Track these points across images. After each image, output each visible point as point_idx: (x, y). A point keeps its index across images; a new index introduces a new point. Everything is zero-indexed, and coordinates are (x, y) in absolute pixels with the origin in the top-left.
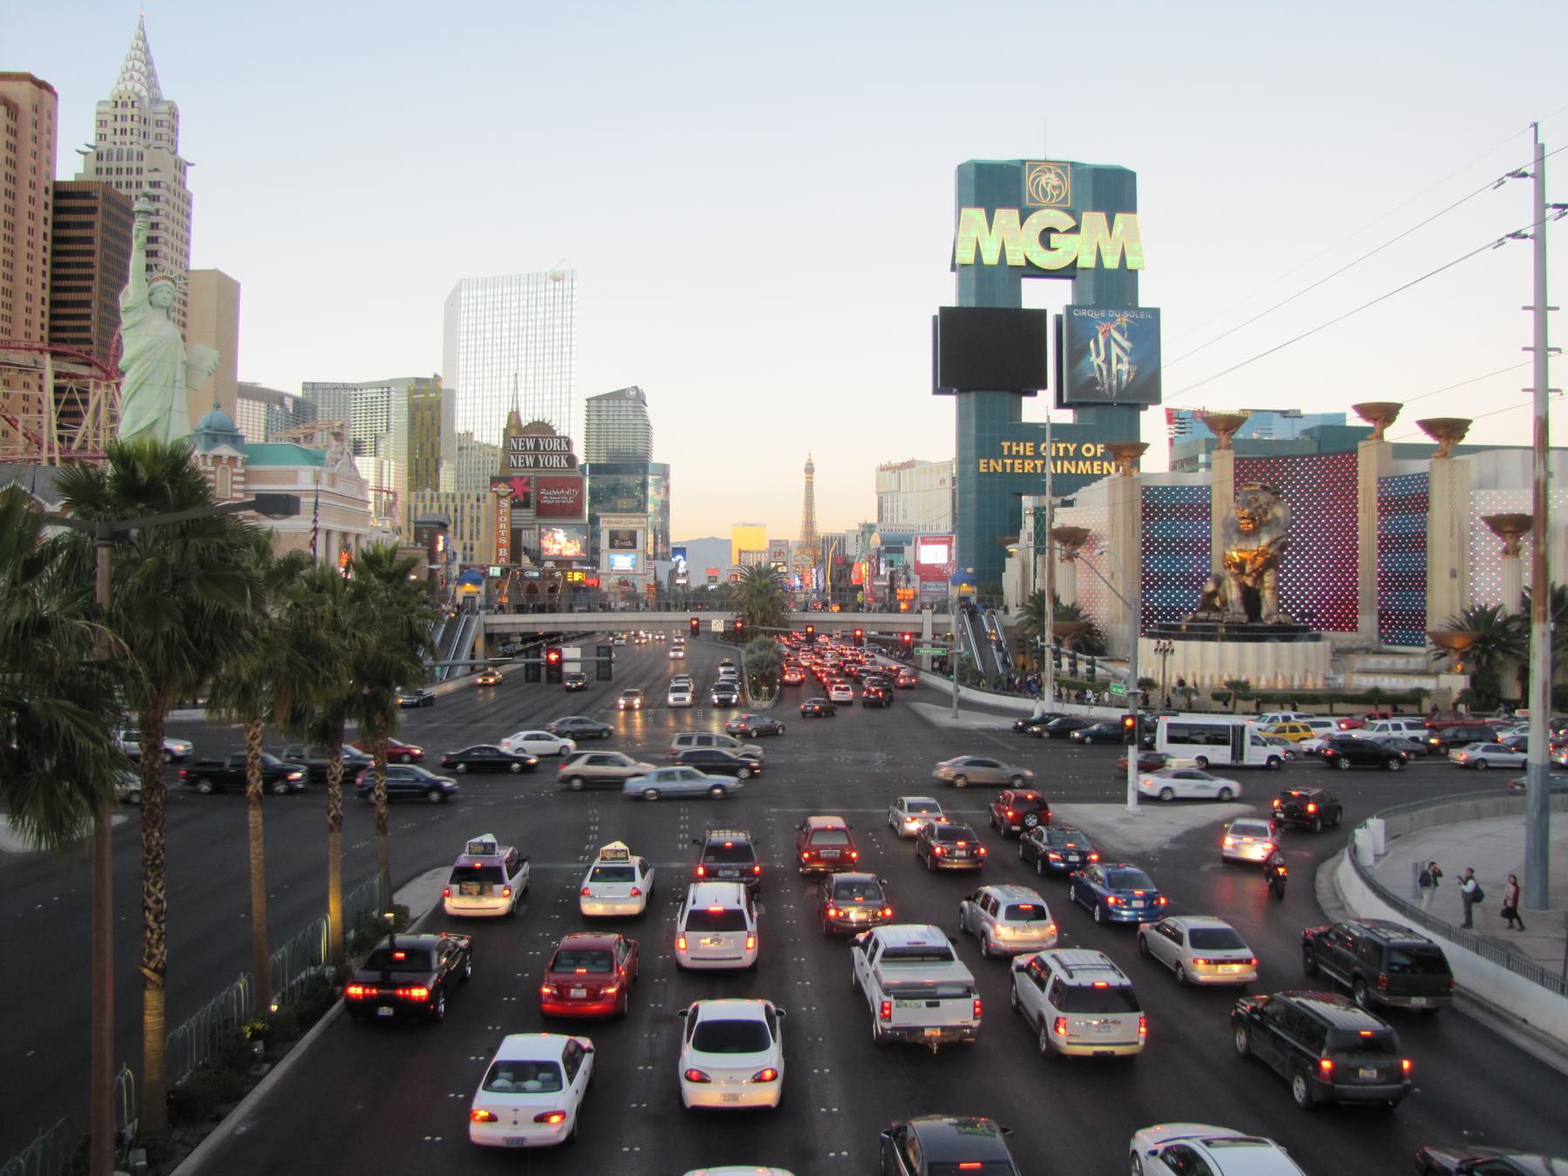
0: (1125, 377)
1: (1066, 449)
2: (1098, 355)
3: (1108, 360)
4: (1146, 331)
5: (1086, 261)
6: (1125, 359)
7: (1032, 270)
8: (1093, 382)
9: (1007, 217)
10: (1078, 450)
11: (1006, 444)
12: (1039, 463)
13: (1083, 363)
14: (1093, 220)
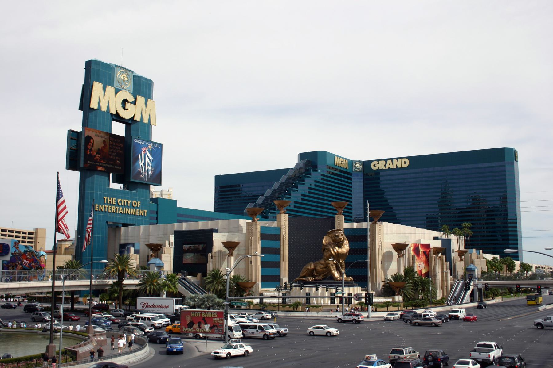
0: (150, 173)
1: (127, 202)
3: (144, 164)
4: (157, 151)
5: (137, 118)
6: (150, 164)
7: (118, 118)
9: (110, 90)
10: (131, 204)
11: (106, 198)
12: (118, 208)
13: (137, 164)
14: (141, 100)
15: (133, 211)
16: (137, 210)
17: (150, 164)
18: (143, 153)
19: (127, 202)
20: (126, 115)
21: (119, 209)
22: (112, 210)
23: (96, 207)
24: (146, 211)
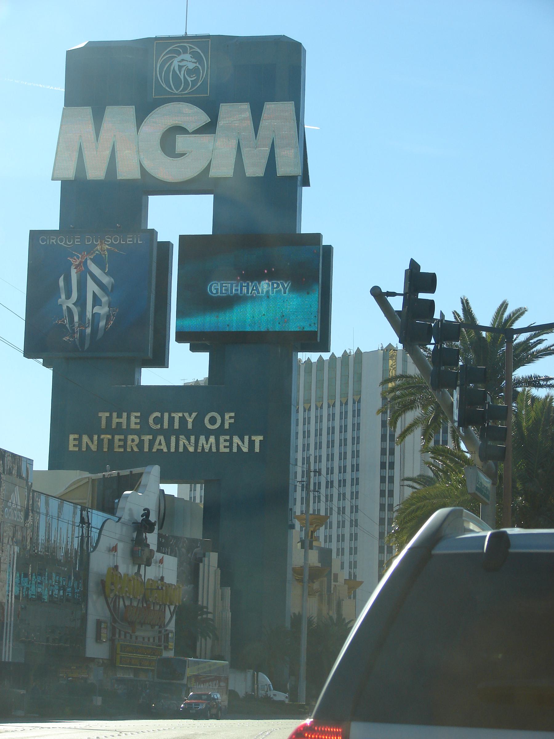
1: (183, 420)
10: (199, 421)
12: (147, 438)
15: (208, 444)
16: (222, 438)
19: (183, 420)
21: (152, 443)
22: (125, 446)
23: (72, 442)
24: (258, 439)
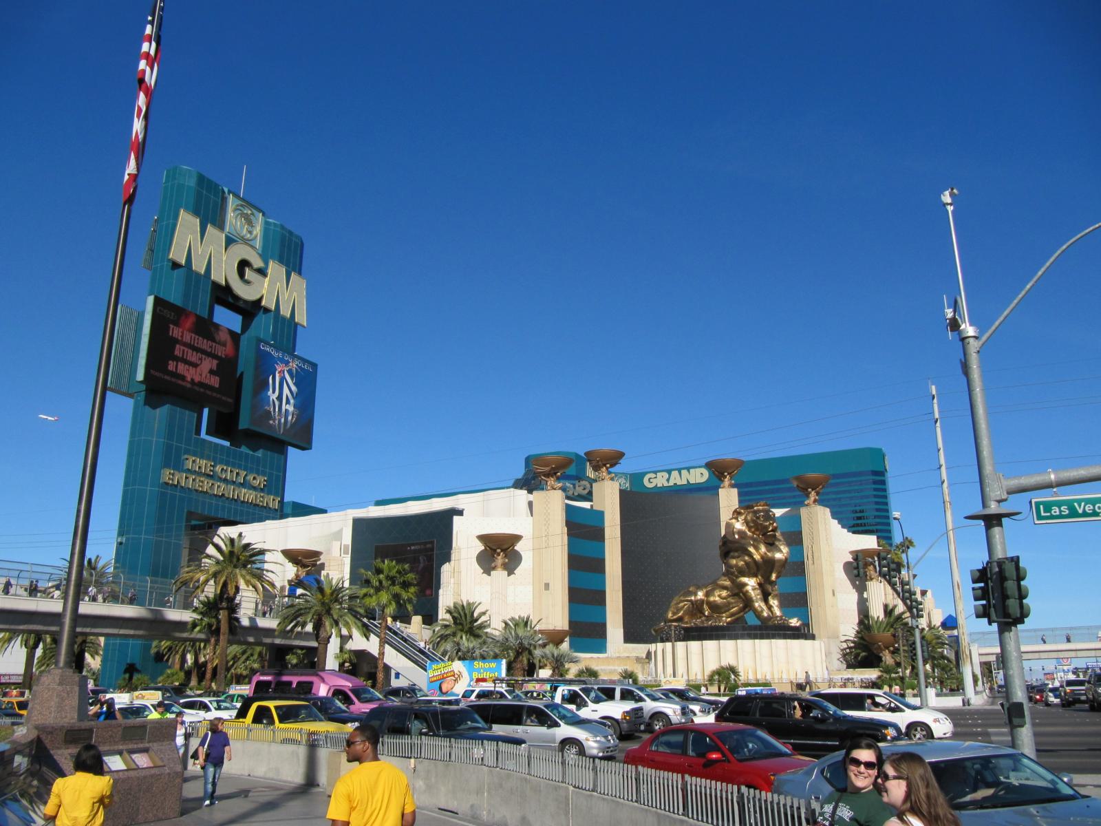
0: (290, 418)
2: (274, 392)
3: (280, 398)
6: (292, 401)
8: (268, 415)
14: (276, 269)
17: (292, 401)
18: (277, 375)
20: (245, 292)
